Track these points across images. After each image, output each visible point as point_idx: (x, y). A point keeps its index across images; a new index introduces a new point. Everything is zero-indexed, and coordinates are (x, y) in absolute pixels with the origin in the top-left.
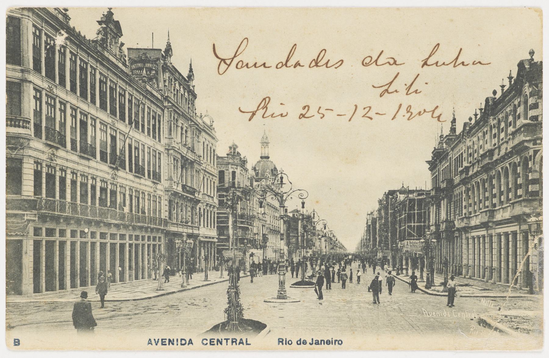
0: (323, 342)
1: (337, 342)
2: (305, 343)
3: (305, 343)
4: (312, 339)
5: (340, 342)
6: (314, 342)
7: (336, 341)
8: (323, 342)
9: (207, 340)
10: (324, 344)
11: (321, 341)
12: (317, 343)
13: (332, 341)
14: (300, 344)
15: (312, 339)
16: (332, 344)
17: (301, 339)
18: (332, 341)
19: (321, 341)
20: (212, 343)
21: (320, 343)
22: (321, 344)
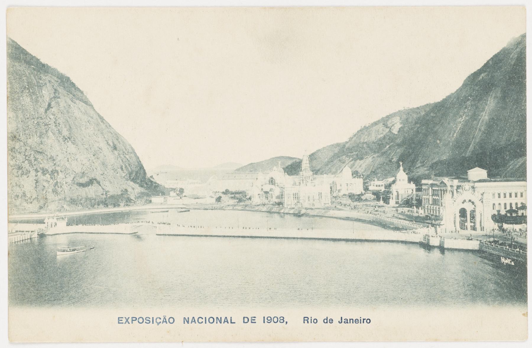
0: (351, 321)
1: (365, 321)
2: (331, 321)
4: (342, 318)
5: (368, 321)
6: (343, 321)
7: (364, 319)
8: (351, 321)
10: (353, 323)
11: (350, 320)
12: (346, 321)
13: (361, 320)
14: (327, 322)
15: (342, 318)
16: (361, 323)
17: (327, 317)
18: (361, 320)
19: (350, 320)
20: (253, 321)
21: (349, 321)
22: (350, 323)
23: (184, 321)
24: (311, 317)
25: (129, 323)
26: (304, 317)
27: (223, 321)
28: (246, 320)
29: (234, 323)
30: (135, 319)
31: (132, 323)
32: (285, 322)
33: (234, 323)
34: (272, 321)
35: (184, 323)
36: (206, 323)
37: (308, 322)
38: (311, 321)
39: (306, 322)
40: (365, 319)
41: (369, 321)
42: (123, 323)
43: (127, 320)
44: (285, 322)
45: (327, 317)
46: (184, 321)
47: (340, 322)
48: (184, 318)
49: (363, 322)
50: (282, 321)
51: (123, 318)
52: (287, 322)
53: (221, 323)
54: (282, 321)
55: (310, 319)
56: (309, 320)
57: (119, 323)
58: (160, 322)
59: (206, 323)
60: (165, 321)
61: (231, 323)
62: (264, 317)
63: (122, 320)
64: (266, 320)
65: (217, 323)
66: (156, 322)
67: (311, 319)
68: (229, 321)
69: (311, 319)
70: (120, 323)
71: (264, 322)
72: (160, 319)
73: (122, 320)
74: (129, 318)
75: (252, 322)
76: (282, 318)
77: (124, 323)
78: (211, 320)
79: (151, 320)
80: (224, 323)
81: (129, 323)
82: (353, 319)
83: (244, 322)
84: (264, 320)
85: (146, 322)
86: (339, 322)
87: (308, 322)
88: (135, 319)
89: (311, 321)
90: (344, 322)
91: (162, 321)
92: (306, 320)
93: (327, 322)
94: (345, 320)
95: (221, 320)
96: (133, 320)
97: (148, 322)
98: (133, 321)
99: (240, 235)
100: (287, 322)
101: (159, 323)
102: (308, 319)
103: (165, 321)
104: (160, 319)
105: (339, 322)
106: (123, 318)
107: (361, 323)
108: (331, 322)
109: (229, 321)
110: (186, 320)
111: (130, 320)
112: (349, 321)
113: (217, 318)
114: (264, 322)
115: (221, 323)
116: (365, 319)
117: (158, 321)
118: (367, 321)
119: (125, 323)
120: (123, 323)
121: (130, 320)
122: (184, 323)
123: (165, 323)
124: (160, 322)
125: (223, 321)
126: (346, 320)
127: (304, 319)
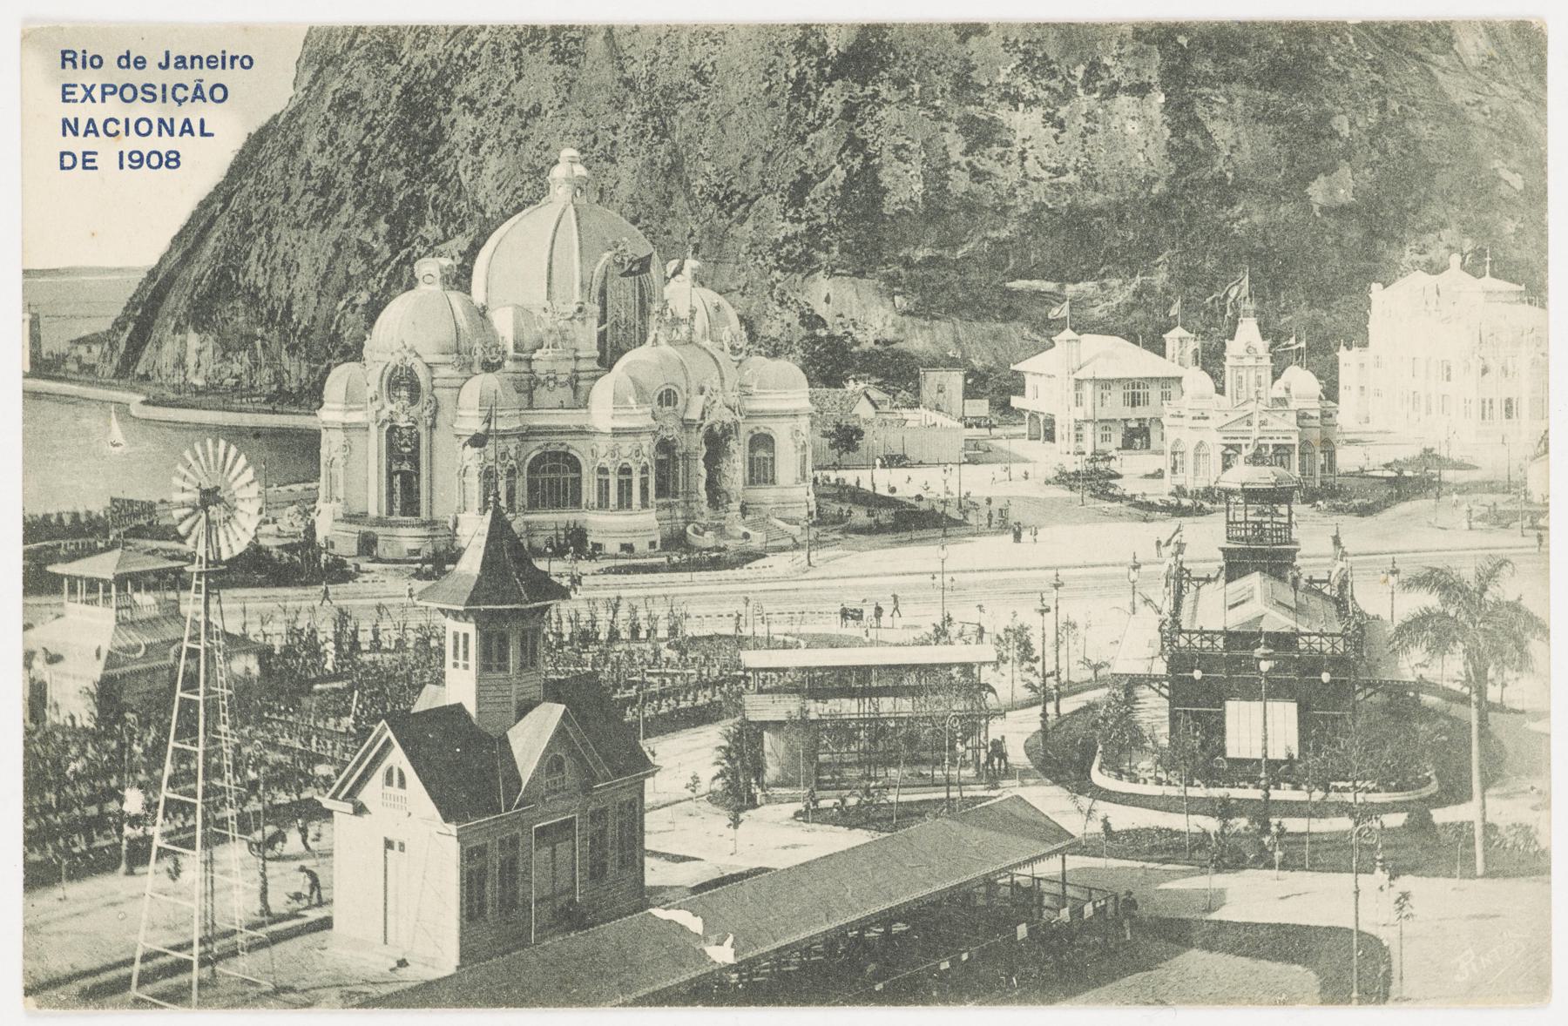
0: (197, 61)
8: (197, 61)
11: (193, 58)
19: (193, 58)
21: (188, 63)
22: (192, 67)
25: (93, 101)
30: (111, 90)
31: (103, 100)
42: (75, 101)
43: (89, 92)
57: (64, 100)
63: (73, 93)
66: (174, 98)
72: (186, 88)
73: (73, 93)
79: (158, 92)
81: (93, 101)
88: (111, 90)
91: (190, 94)
96: (104, 94)
104: (186, 88)
111: (97, 93)
112: (188, 63)
119: (83, 101)
120: (75, 101)
121: (97, 93)
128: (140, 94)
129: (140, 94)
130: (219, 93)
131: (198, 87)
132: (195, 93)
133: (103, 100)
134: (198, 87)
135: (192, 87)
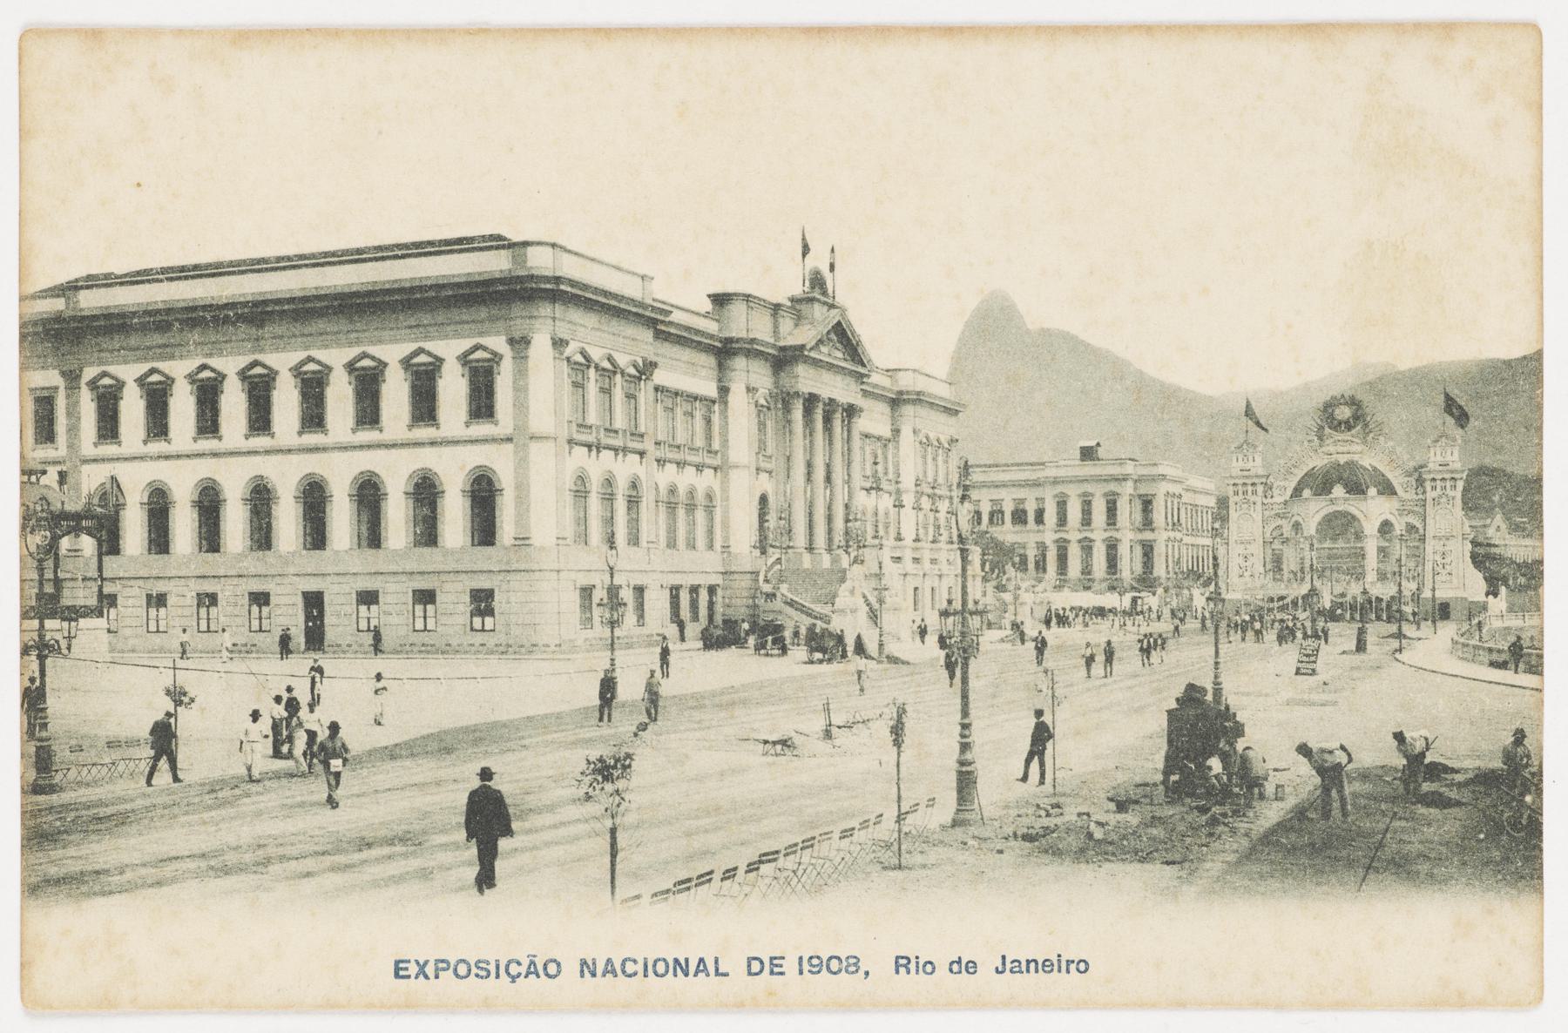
0: (1032, 965)
1: (1073, 967)
2: (971, 967)
3: (971, 967)
4: (1004, 957)
6: (1008, 966)
7: (1069, 962)
8: (1032, 965)
9: (635, 961)
10: (1037, 971)
11: (1028, 962)
13: (1059, 961)
14: (960, 972)
15: (1004, 957)
16: (1059, 971)
17: (960, 958)
18: (1059, 961)
19: (1028, 962)
22: (1028, 971)
23: (582, 971)
24: (917, 958)
25: (426, 977)
26: (897, 958)
27: (692, 969)
28: (756, 966)
29: (726, 975)
30: (444, 965)
31: (437, 977)
32: (861, 973)
33: (726, 975)
34: (824, 968)
35: (582, 976)
36: (645, 976)
37: (908, 972)
38: (917, 967)
39: (902, 970)
40: (1073, 962)
41: (1083, 966)
42: (409, 977)
43: (422, 968)
44: (861, 973)
45: (960, 958)
46: (582, 971)
47: (1000, 969)
48: (584, 963)
49: (1068, 971)
50: (852, 969)
51: (409, 961)
52: (867, 973)
53: (594, 975)
54: (852, 969)
55: (913, 961)
56: (912, 966)
58: (519, 975)
59: (645, 976)
60: (532, 969)
61: (717, 973)
62: (801, 958)
63: (406, 969)
64: (806, 967)
65: (675, 975)
66: (508, 974)
67: (917, 963)
68: (711, 969)
69: (917, 963)
70: (403, 977)
71: (801, 972)
72: (519, 963)
73: (406, 969)
74: (426, 962)
75: (772, 973)
76: (852, 961)
77: (413, 976)
78: (661, 968)
79: (492, 968)
80: (695, 975)
81: (426, 977)
82: (1035, 961)
83: (750, 973)
84: (800, 964)
85: (477, 975)
86: (997, 968)
87: (908, 972)
88: (444, 965)
89: (917, 967)
90: (1011, 971)
91: (523, 969)
92: (905, 966)
93: (960, 972)
94: (1013, 962)
95: (687, 965)
96: (437, 969)
97: (483, 973)
98: (441, 974)
99: (94, 272)
100: (867, 973)
101: (514, 979)
102: (909, 962)
103: (532, 971)
104: (519, 963)
105: (997, 968)
106: (409, 961)
107: (1059, 971)
108: (971, 970)
109: (711, 969)
110: (587, 968)
112: (1024, 969)
113: (676, 961)
114: (801, 972)
115: (594, 975)
116: (1073, 962)
117: (514, 969)
118: (1078, 970)
119: (416, 978)
120: (409, 977)
121: (430, 970)
122: (582, 976)
123: (532, 977)
124: (519, 975)
125: (692, 969)
126: (1017, 964)
127: (896, 962)
128: (474, 970)
129: (474, 970)
130: (552, 969)
131: (532, 963)
132: (529, 968)
133: (437, 977)
134: (532, 963)
135: (526, 963)
